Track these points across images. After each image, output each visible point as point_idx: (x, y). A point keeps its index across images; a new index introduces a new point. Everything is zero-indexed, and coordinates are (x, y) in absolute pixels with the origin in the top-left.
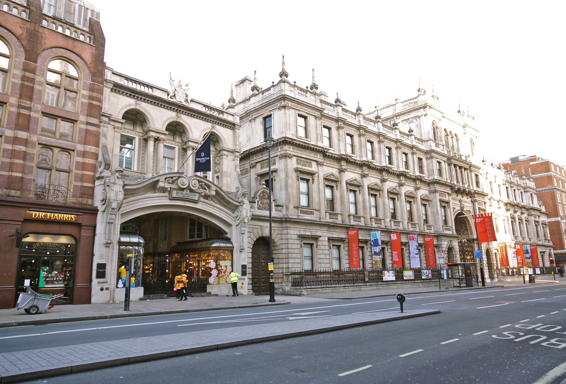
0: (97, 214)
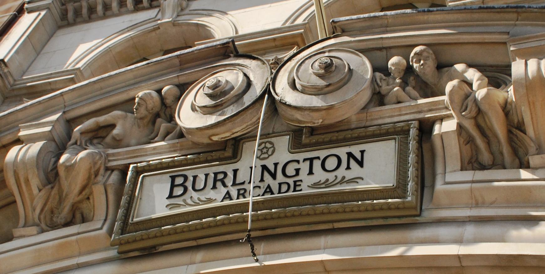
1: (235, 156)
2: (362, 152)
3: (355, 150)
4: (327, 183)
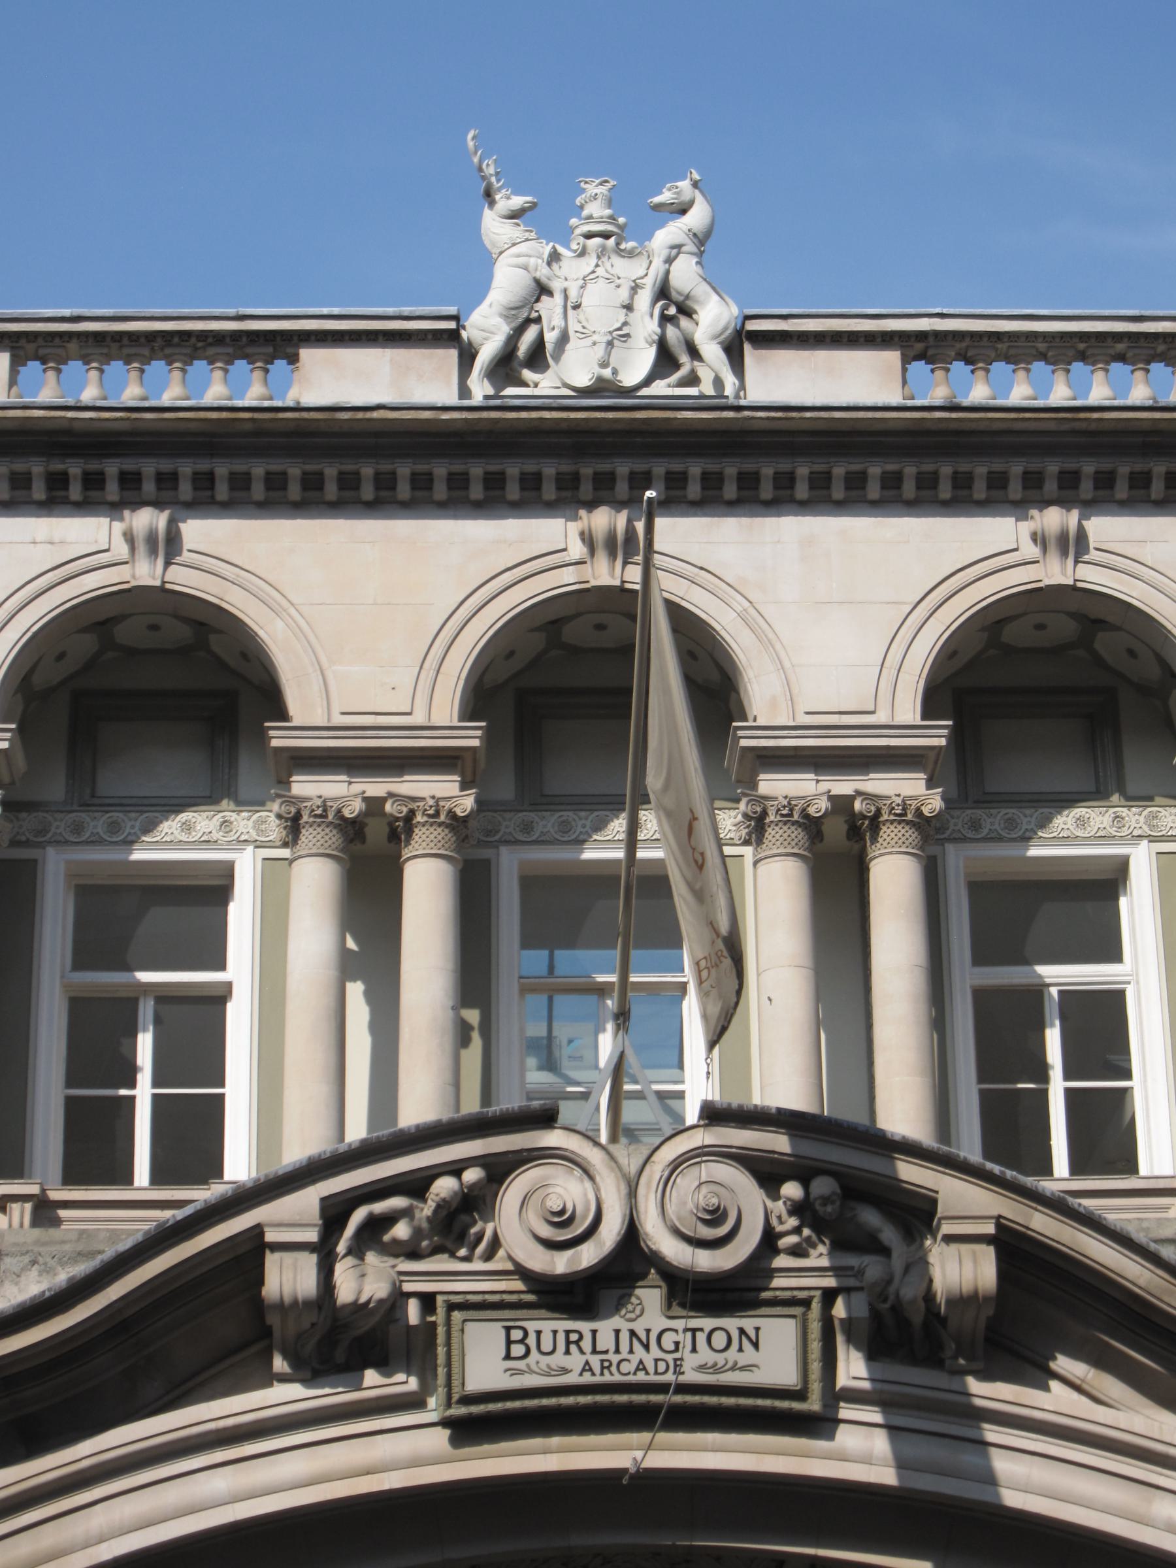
2: (757, 1329)
4: (715, 1369)
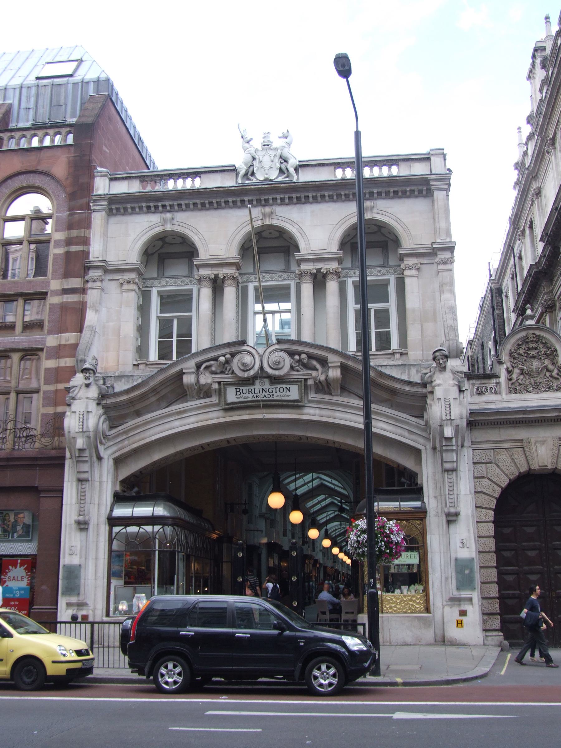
0: (63, 465)
1: (253, 384)
3: (288, 386)
